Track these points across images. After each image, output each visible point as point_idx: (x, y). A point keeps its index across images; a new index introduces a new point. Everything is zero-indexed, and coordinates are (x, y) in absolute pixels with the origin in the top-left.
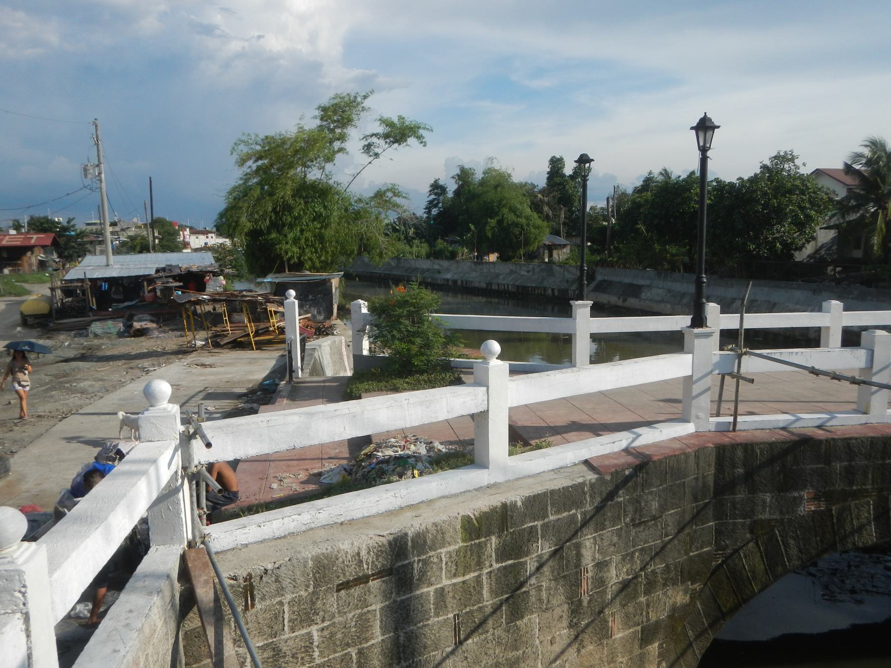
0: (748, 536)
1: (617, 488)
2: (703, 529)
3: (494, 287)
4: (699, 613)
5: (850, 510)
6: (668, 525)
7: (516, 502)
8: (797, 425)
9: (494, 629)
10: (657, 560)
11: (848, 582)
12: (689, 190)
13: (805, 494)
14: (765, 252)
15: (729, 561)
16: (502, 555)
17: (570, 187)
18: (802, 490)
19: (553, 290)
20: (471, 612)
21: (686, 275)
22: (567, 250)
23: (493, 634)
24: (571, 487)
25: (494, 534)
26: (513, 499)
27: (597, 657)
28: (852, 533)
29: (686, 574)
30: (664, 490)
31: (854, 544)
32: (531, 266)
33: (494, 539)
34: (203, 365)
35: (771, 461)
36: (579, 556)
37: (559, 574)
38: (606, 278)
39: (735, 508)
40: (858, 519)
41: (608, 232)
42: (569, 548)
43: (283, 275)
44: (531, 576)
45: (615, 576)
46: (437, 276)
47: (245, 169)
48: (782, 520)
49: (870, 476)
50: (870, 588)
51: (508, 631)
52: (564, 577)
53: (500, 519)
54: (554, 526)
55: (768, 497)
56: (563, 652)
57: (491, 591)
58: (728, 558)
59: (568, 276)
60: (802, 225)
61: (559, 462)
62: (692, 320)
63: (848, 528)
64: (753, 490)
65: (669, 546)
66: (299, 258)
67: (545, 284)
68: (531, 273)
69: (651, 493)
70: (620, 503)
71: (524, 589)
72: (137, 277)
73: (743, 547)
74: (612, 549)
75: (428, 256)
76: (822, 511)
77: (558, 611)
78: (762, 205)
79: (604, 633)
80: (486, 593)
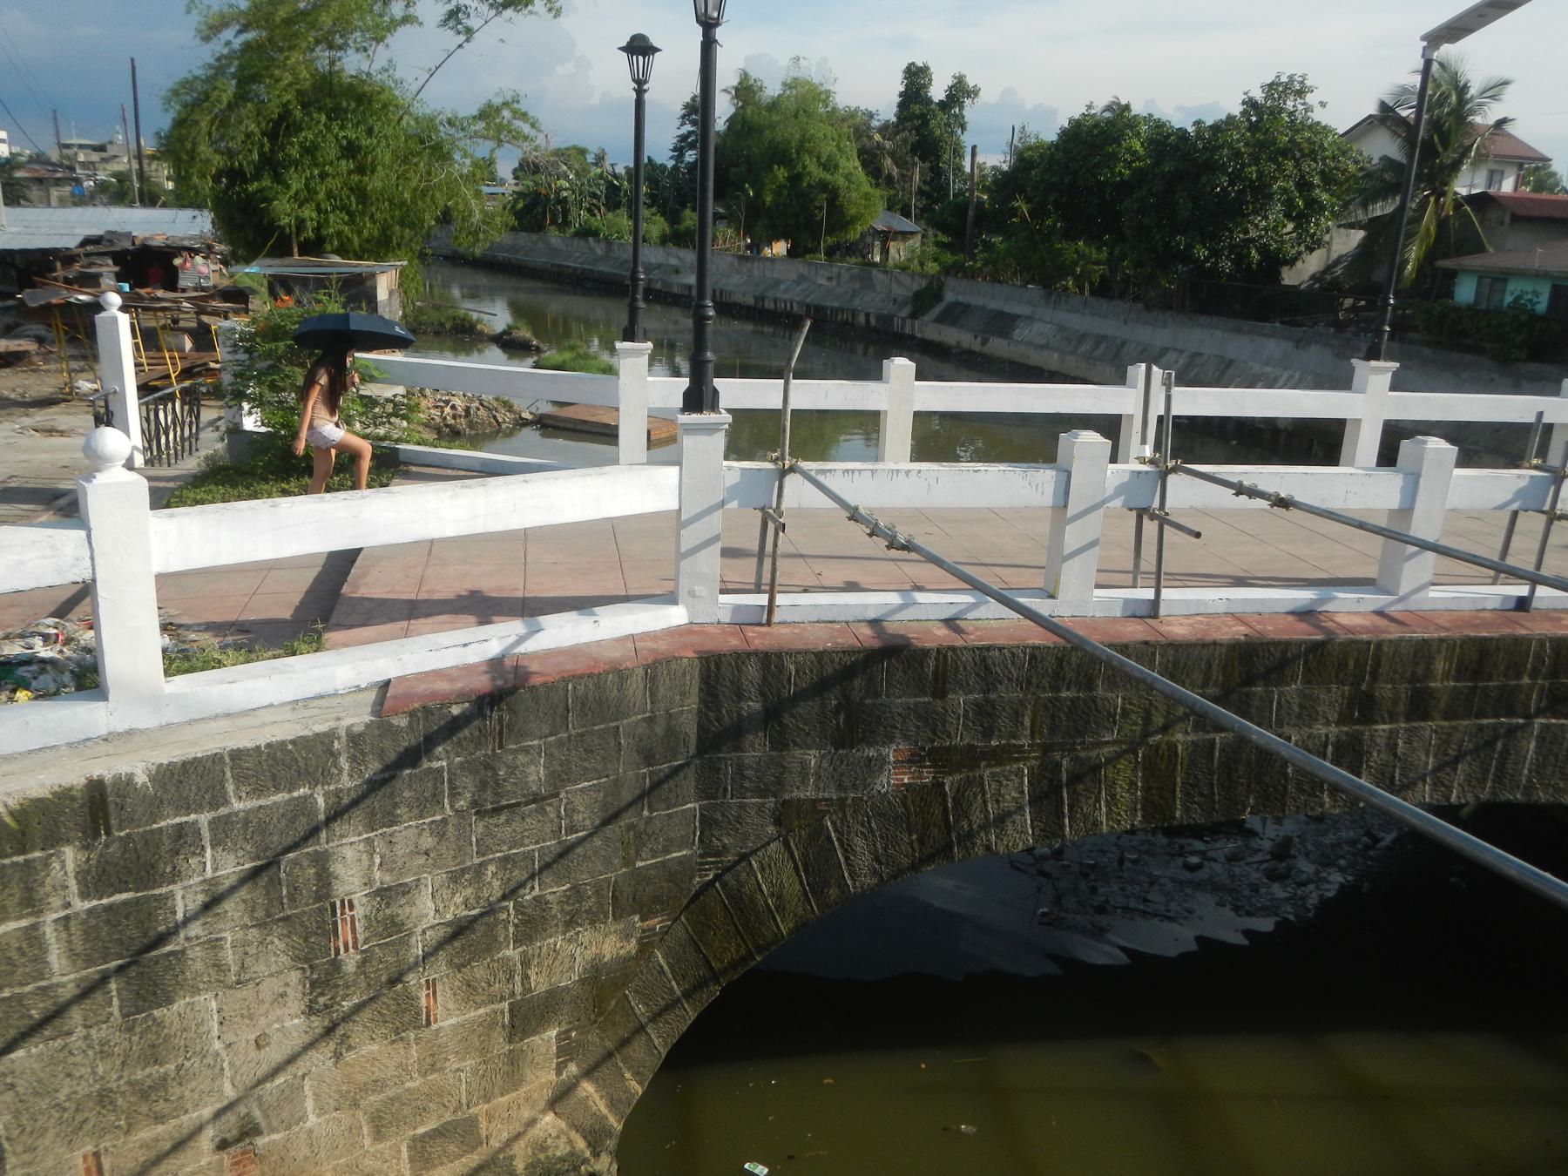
0: (771, 829)
1: (428, 744)
2: (669, 816)
3: (769, 305)
4: (662, 972)
5: (982, 785)
6: (574, 810)
7: (130, 777)
8: (905, 615)
9: (86, 1026)
10: (548, 877)
11: (1101, 890)
12: (1117, 140)
13: (891, 753)
14: (1226, 265)
15: (728, 877)
16: (93, 882)
17: (936, 125)
18: (884, 744)
19: (867, 315)
20: (19, 998)
21: (1092, 300)
22: (915, 242)
23: (86, 1037)
24: (293, 742)
25: (68, 842)
26: (129, 770)
27: (391, 1064)
28: (984, 827)
29: (625, 902)
30: (560, 743)
31: (988, 848)
32: (835, 270)
33: (70, 855)
34: (51, 432)
35: (820, 687)
36: (325, 879)
37: (268, 915)
38: (961, 298)
39: (743, 777)
40: (998, 801)
41: (971, 213)
42: (295, 862)
43: (287, 261)
44: (187, 921)
45: (428, 911)
46: (674, 279)
47: (217, 47)
48: (842, 801)
49: (1027, 722)
50: (1133, 904)
51: (130, 1030)
52: (287, 919)
53: (96, 806)
54: (246, 822)
55: (812, 758)
56: (291, 1060)
57: (72, 954)
58: (727, 870)
59: (898, 291)
60: (1304, 214)
61: (335, 680)
62: (687, 395)
63: (977, 818)
64: (780, 743)
65: (579, 850)
66: (318, 229)
67: (856, 303)
68: (834, 283)
69: (526, 750)
70: (440, 771)
71: (168, 948)
72: (45, 252)
73: (758, 849)
74: (421, 860)
75: (664, 240)
76: (925, 786)
77: (270, 987)
78: (1229, 175)
79: (408, 1019)
80: (56, 958)
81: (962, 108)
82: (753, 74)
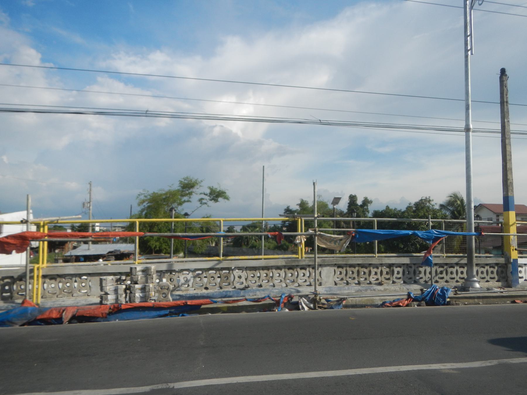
43: (151, 255)
47: (142, 207)
66: (159, 247)
81: (367, 206)
82: (304, 199)
